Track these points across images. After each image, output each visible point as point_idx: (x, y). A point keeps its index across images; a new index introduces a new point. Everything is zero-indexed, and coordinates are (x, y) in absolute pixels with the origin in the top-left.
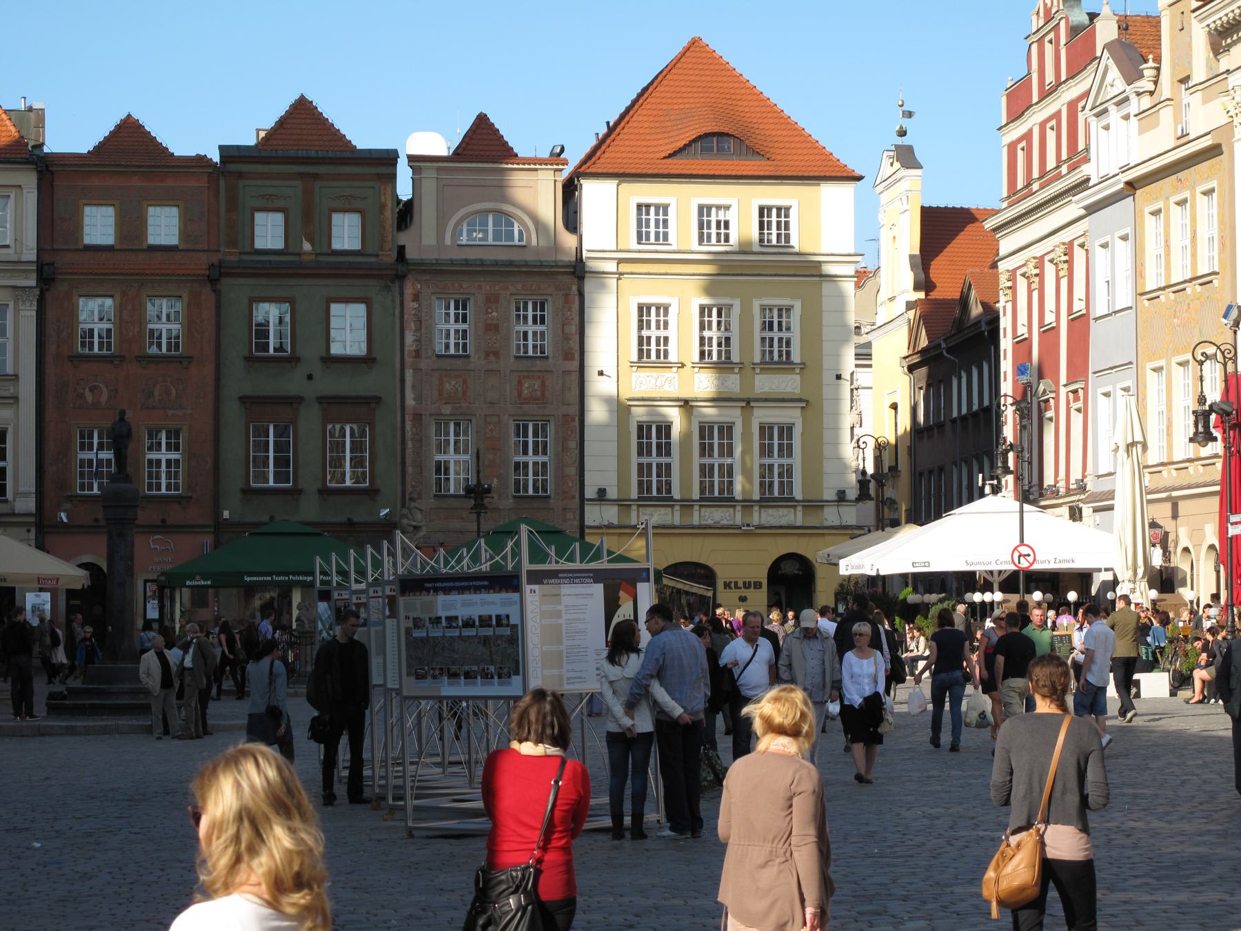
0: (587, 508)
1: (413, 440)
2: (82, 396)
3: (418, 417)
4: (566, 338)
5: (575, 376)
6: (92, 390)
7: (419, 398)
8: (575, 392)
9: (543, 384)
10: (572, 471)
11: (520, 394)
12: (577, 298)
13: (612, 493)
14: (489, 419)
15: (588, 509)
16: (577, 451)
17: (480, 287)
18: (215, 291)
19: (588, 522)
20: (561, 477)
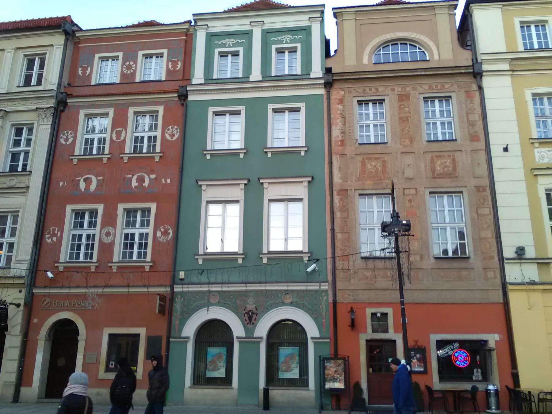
0: (506, 266)
1: (341, 211)
2: (78, 185)
3: (344, 192)
4: (472, 124)
5: (482, 155)
6: (85, 180)
7: (345, 178)
8: (485, 167)
9: (454, 160)
10: (489, 234)
11: (433, 171)
12: (477, 95)
13: (530, 253)
14: (407, 192)
15: (508, 268)
16: (491, 217)
17: (393, 90)
18: (183, 105)
19: (510, 278)
20: (478, 240)
